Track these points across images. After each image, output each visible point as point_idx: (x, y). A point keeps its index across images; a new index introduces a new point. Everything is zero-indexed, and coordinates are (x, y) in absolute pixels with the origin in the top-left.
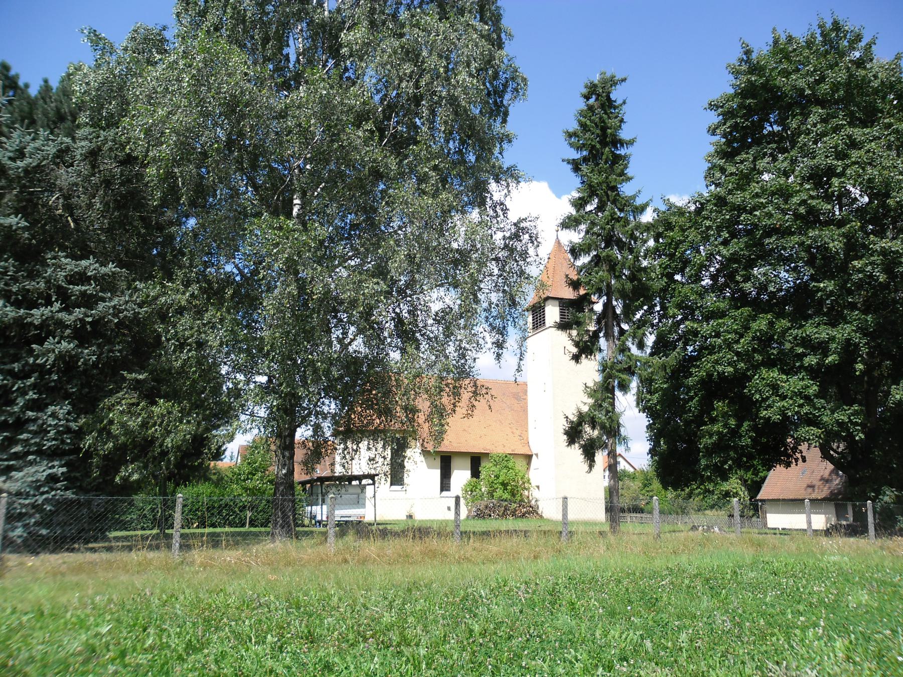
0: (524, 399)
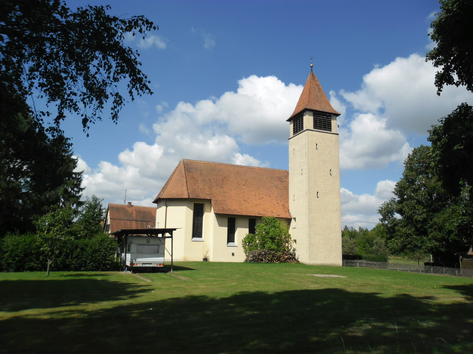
0: (286, 181)
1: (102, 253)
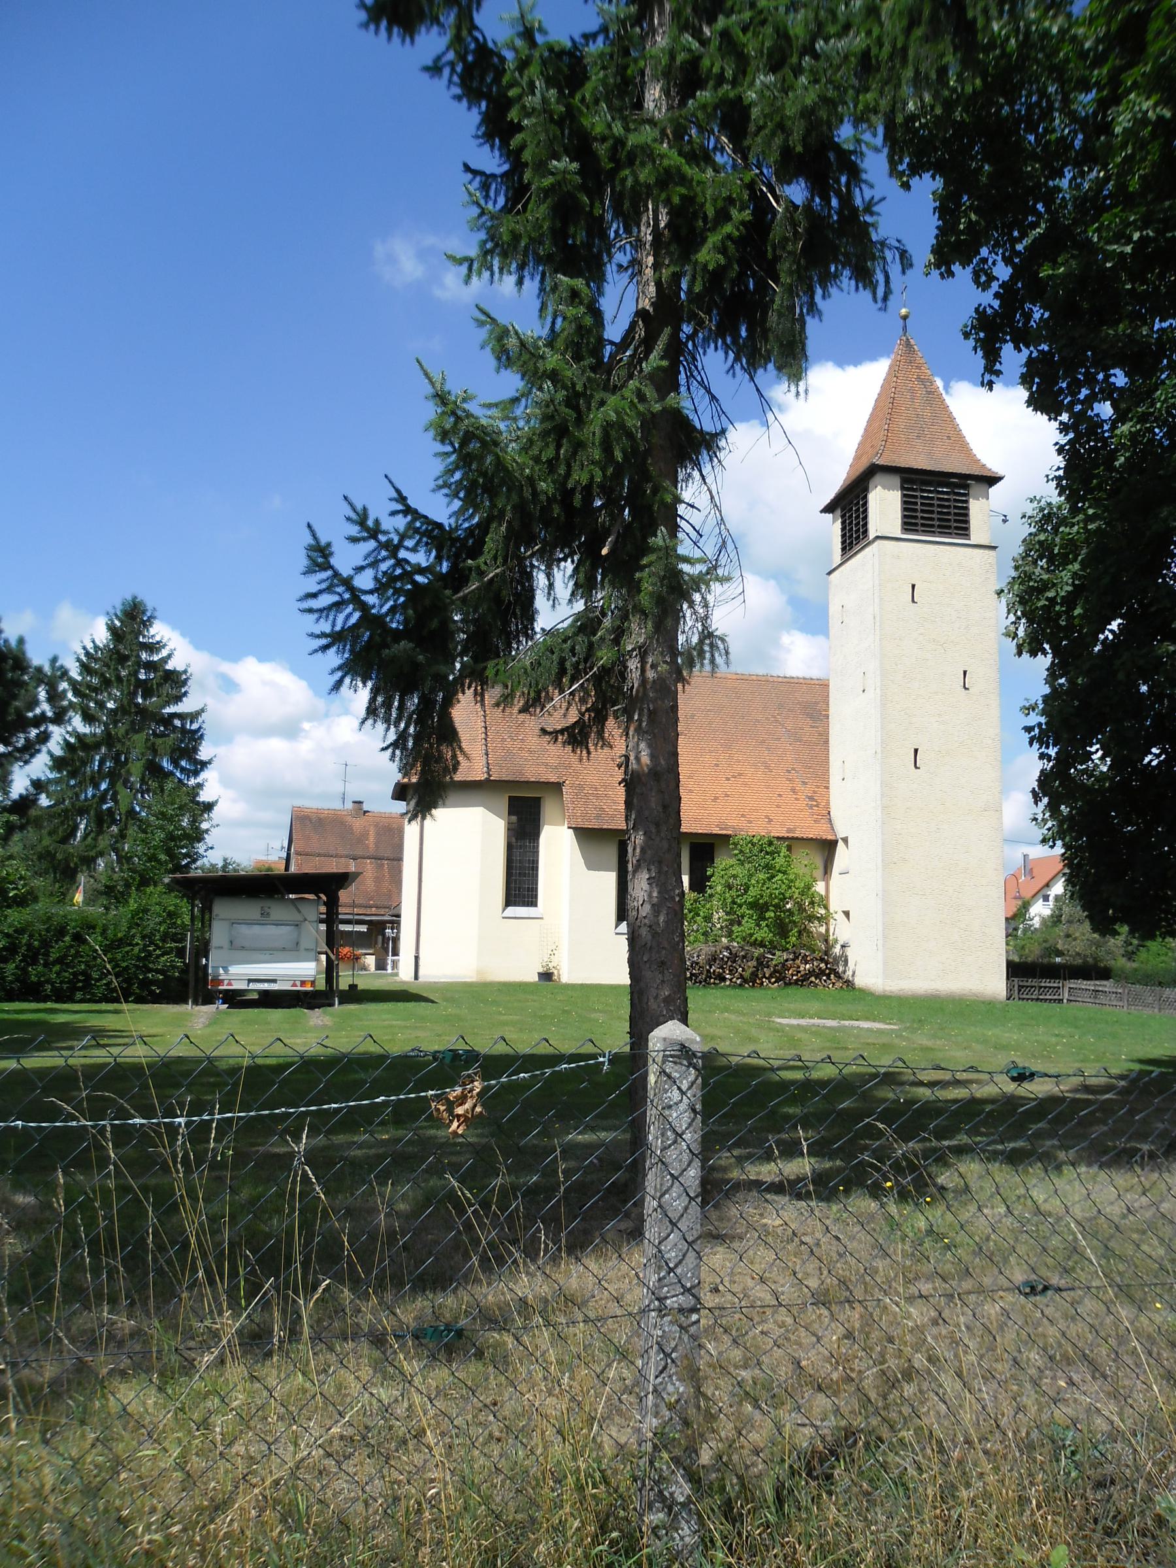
1: (137, 949)
